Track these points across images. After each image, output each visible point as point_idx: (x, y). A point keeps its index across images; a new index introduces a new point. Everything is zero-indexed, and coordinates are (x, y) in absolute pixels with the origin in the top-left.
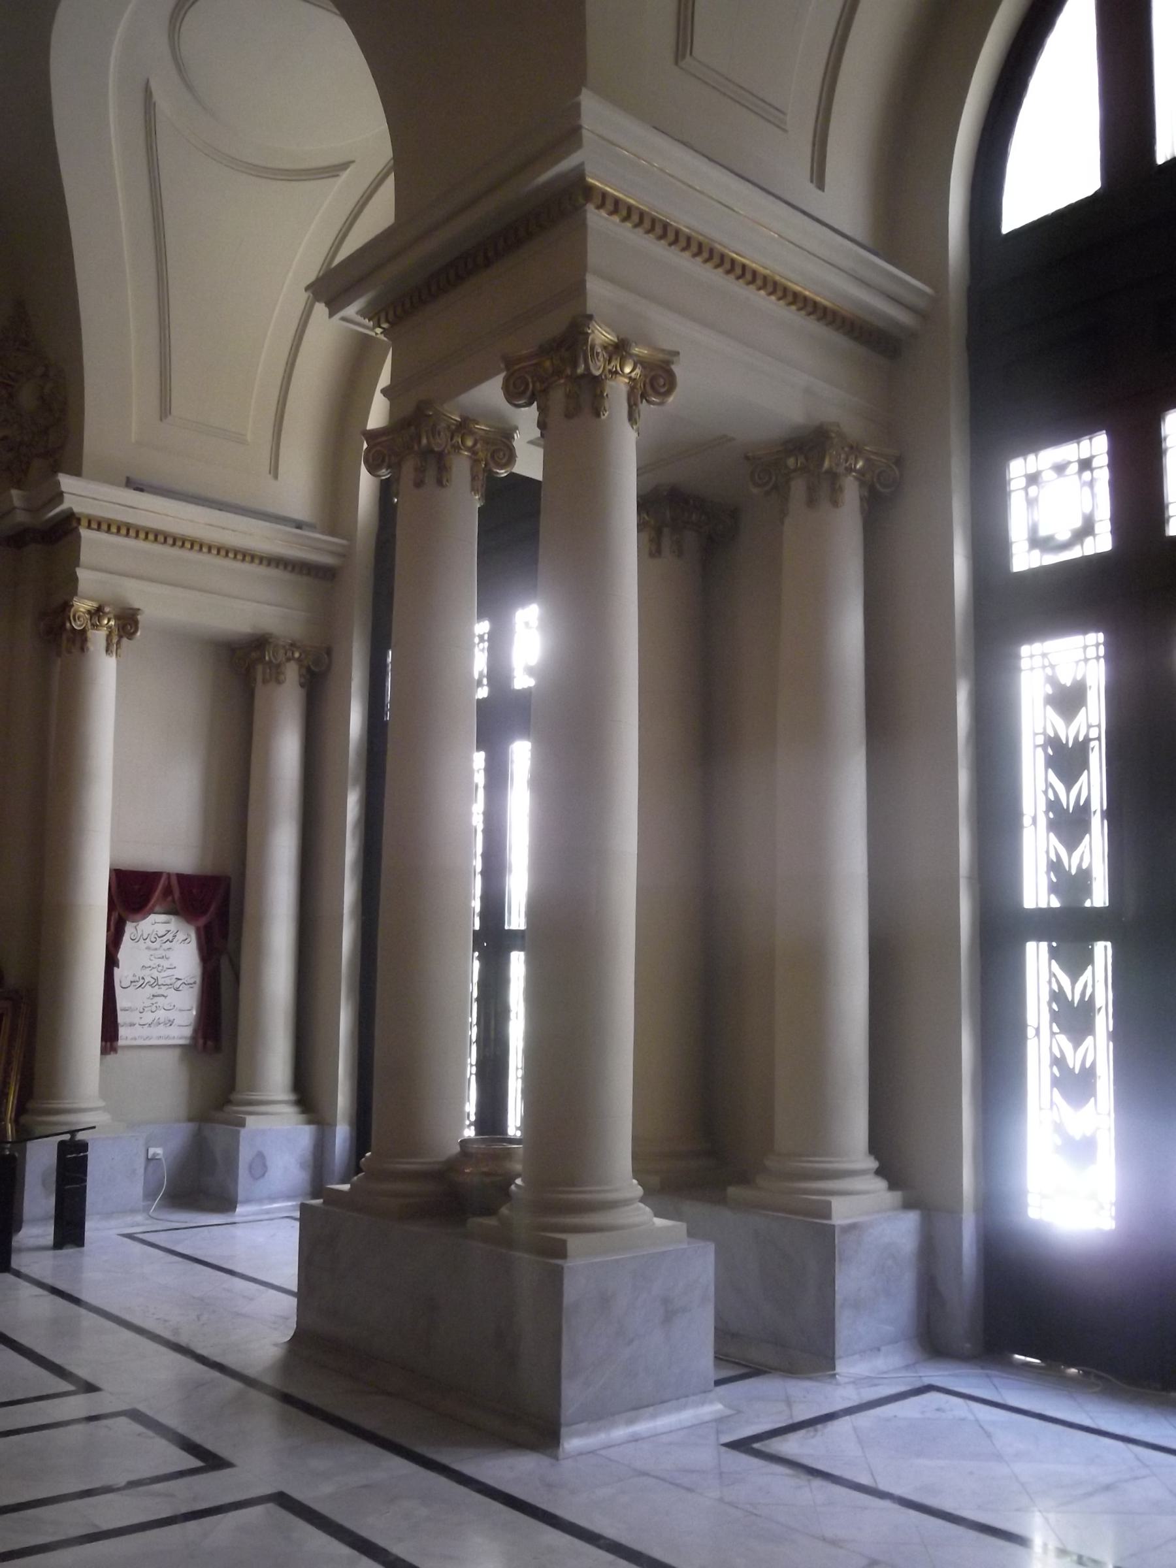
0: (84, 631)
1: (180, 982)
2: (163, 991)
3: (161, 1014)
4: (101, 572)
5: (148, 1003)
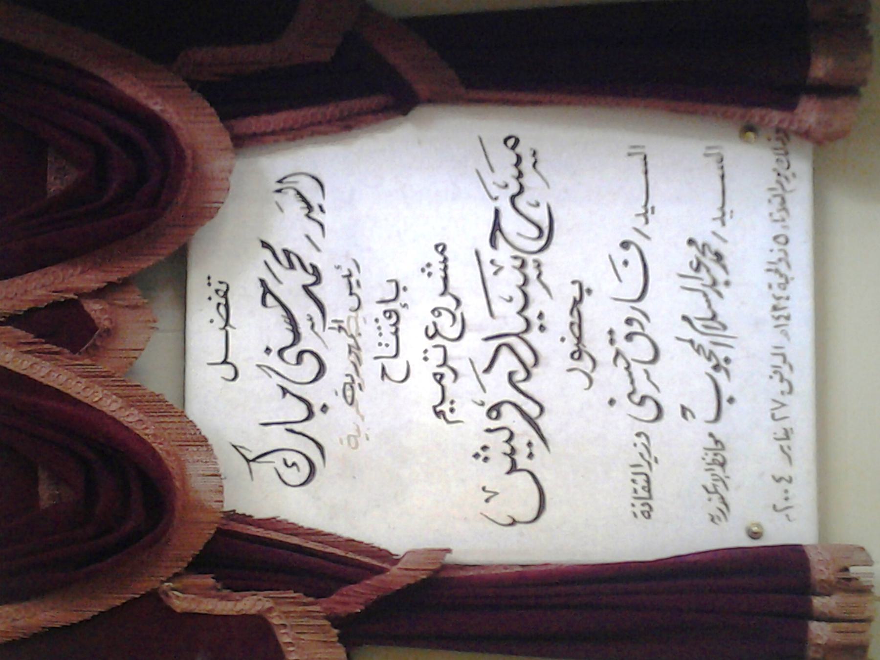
1: (511, 222)
2: (559, 317)
3: (671, 303)
5: (612, 379)
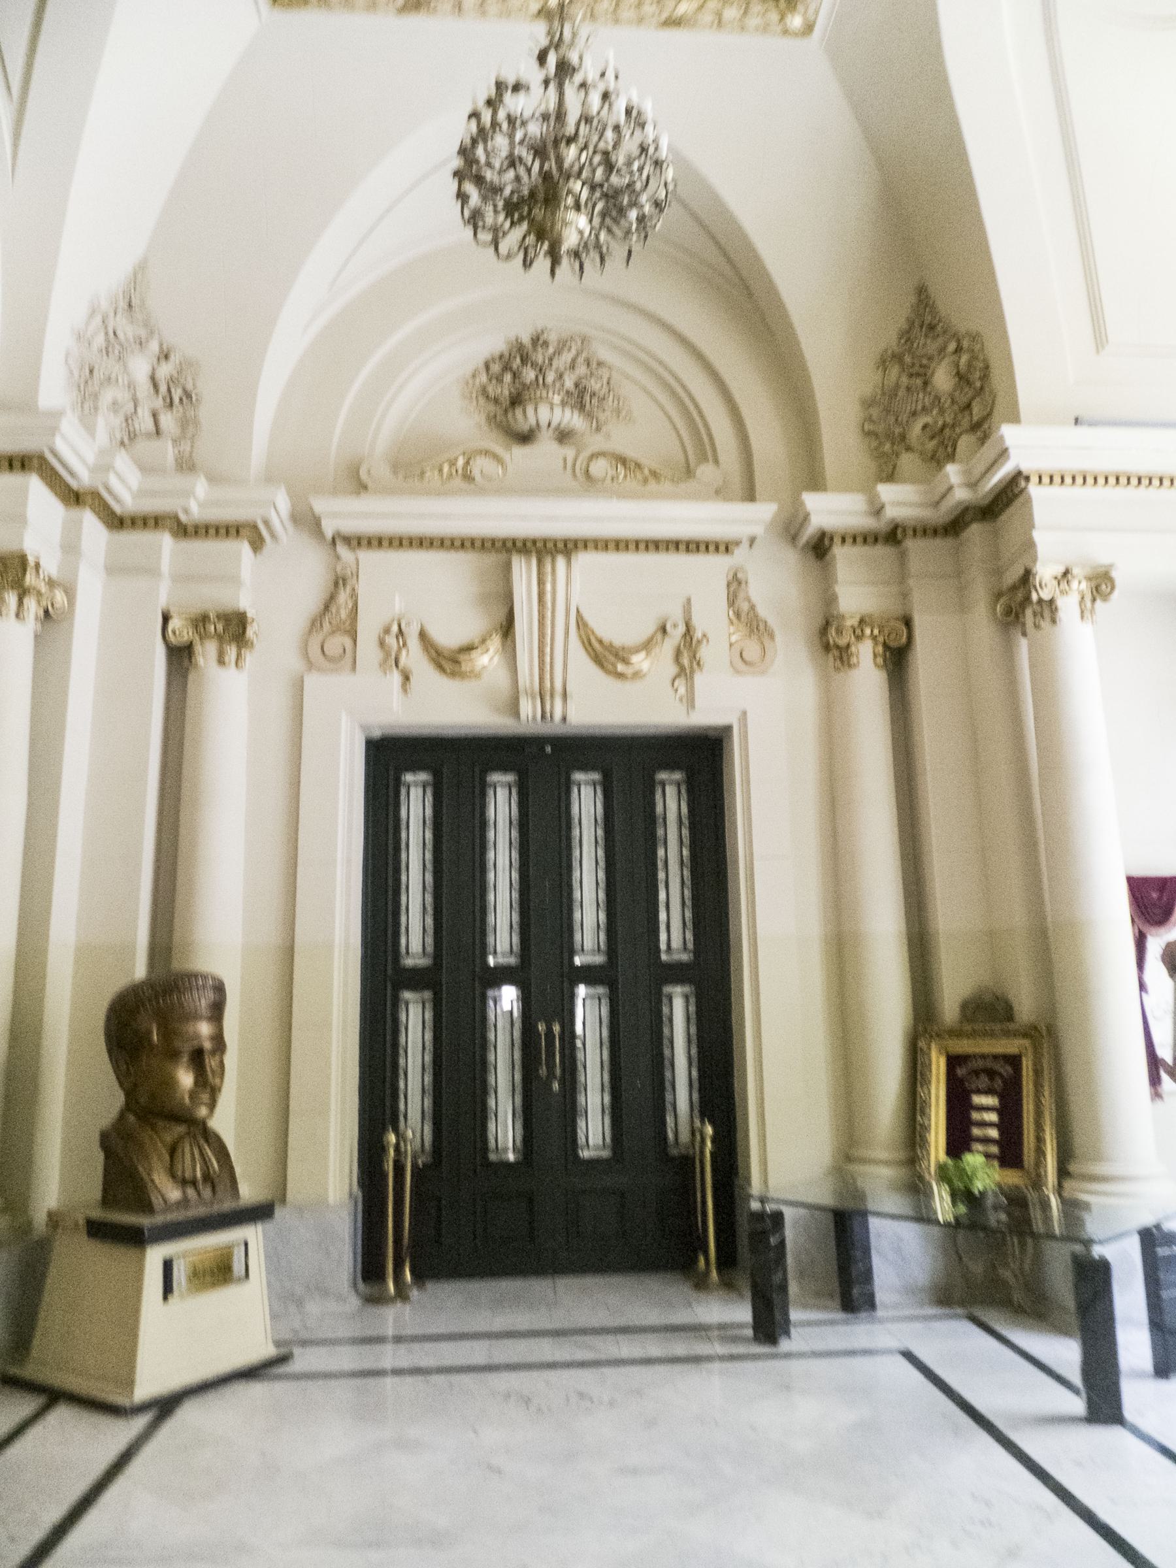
0: (1051, 602)
4: (1058, 533)
